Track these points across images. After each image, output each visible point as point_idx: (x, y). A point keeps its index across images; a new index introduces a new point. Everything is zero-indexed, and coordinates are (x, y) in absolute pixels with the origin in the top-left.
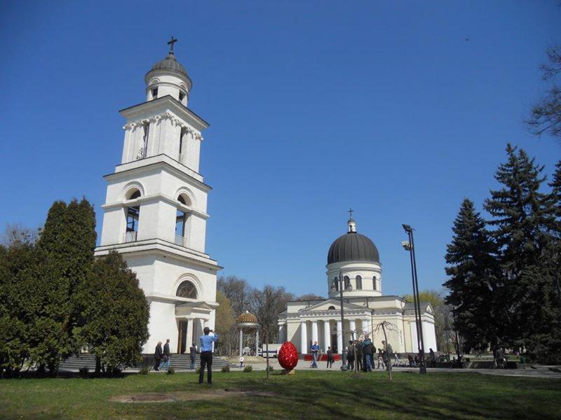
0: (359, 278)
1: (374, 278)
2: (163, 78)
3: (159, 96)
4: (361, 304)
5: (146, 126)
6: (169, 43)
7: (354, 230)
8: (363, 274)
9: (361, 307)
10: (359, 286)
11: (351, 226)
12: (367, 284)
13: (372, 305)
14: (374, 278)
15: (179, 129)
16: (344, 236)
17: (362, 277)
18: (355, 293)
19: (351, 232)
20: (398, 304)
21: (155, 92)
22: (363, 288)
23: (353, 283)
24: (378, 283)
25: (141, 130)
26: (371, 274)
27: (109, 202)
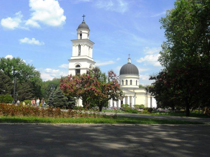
0: (131, 81)
1: (137, 81)
2: (83, 31)
3: (82, 39)
4: (132, 91)
5: (80, 46)
6: (83, 16)
7: (130, 62)
8: (133, 79)
9: (131, 92)
10: (131, 84)
11: (129, 61)
12: (134, 83)
13: (136, 91)
14: (137, 81)
15: (88, 47)
16: (126, 64)
17: (132, 80)
18: (129, 86)
19: (129, 63)
20: (144, 91)
21: (81, 35)
22: (132, 84)
23: (129, 83)
24: (138, 83)
25: (77, 47)
26: (136, 80)
27: (70, 68)
